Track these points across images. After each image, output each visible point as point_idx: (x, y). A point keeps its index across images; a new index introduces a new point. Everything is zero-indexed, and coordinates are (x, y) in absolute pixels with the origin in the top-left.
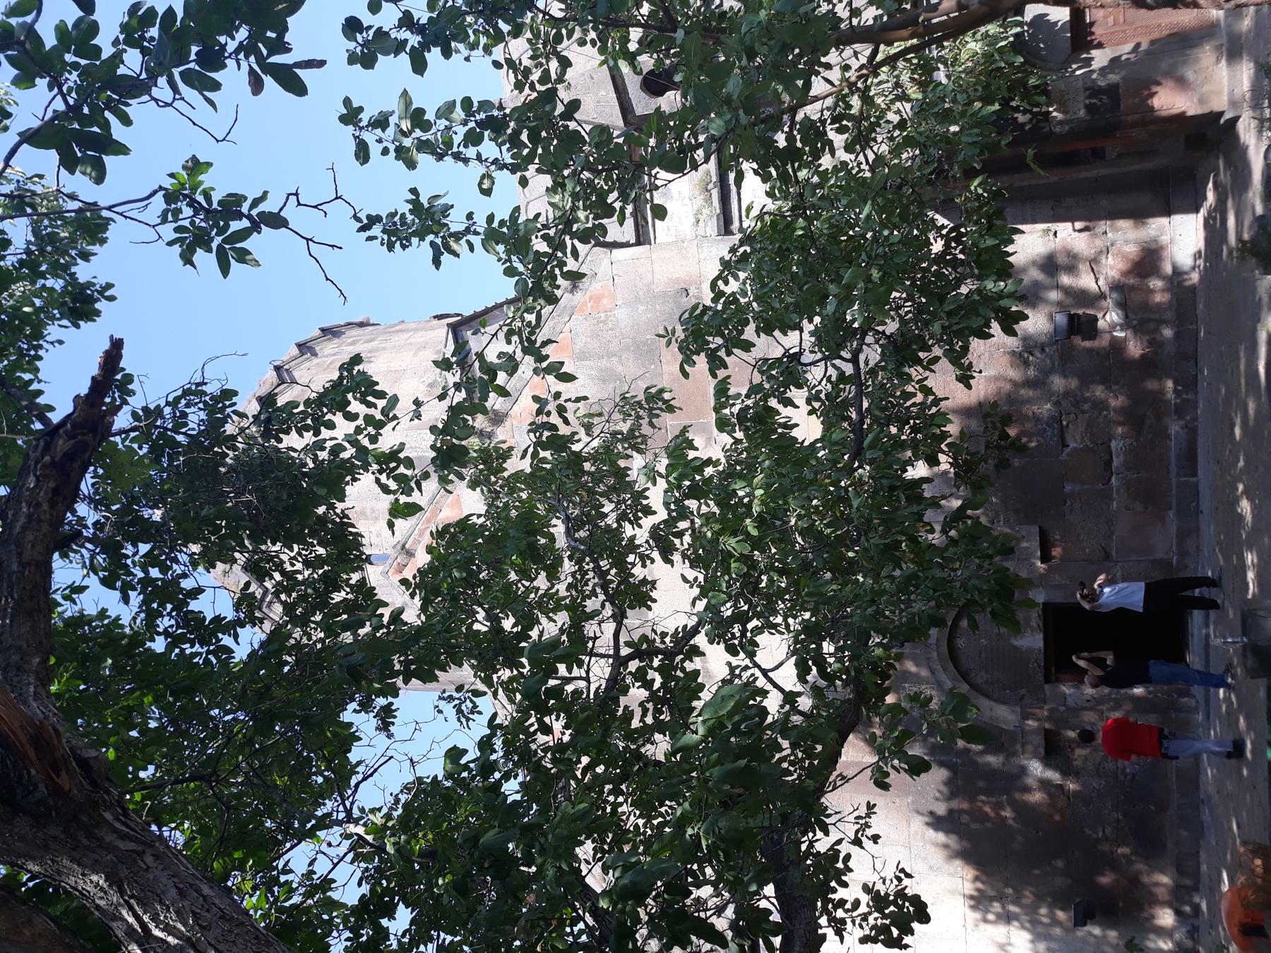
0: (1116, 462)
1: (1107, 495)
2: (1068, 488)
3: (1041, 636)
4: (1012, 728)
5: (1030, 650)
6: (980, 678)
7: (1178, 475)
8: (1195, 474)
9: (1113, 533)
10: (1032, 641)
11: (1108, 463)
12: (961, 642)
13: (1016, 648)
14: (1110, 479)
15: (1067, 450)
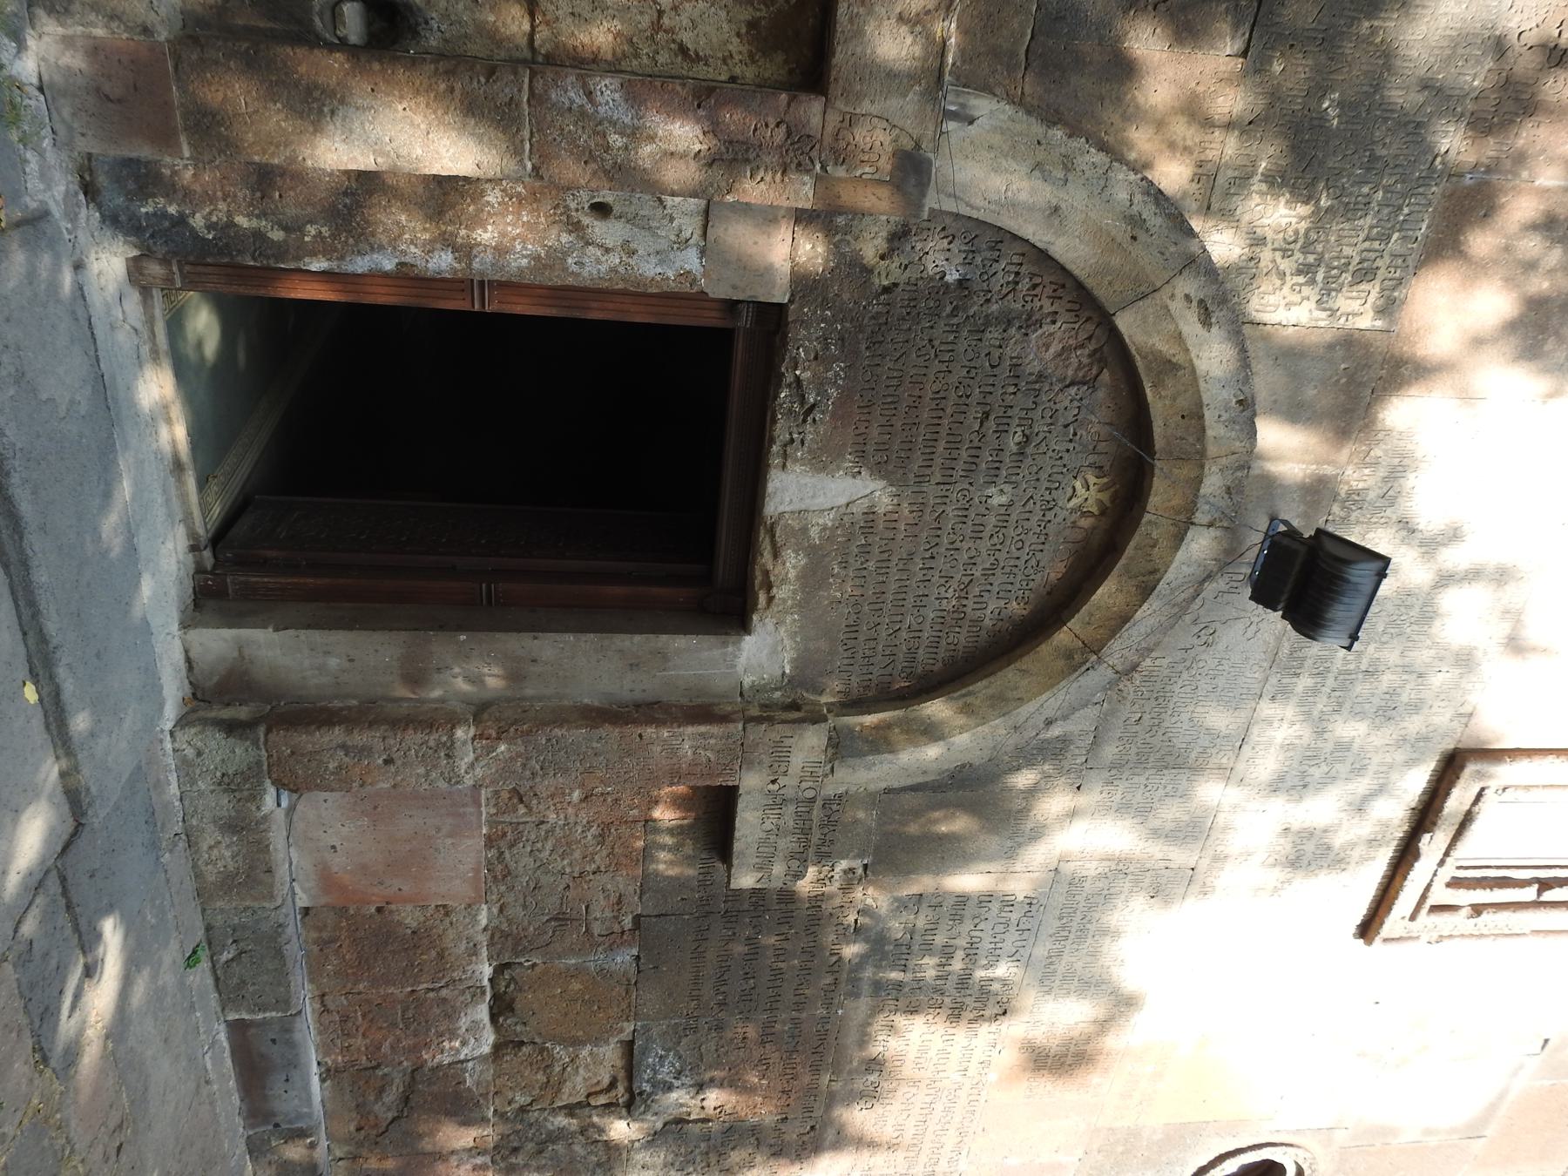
0: (482, 1012)
1: (507, 943)
2: (624, 958)
3: (771, 508)
4: (982, 106)
5: (822, 462)
6: (1051, 344)
7: (286, 1027)
8: (238, 1030)
9: (490, 842)
10: (811, 491)
11: (501, 1007)
12: (1086, 494)
13: (879, 470)
14: (499, 970)
15: (626, 1035)
